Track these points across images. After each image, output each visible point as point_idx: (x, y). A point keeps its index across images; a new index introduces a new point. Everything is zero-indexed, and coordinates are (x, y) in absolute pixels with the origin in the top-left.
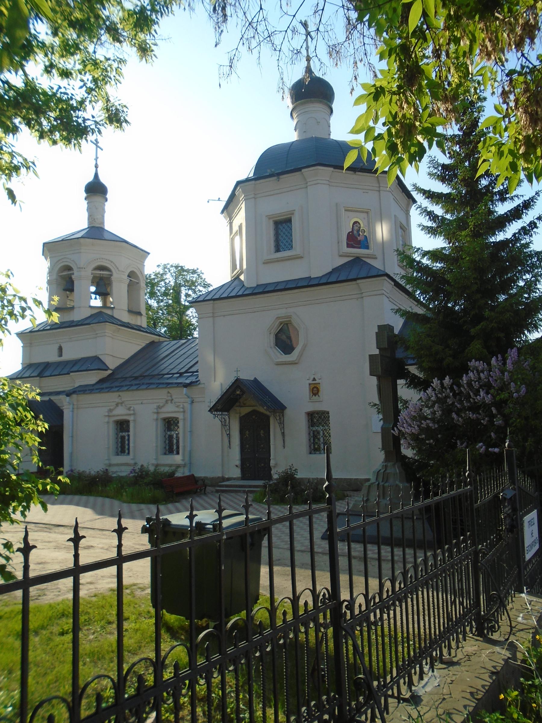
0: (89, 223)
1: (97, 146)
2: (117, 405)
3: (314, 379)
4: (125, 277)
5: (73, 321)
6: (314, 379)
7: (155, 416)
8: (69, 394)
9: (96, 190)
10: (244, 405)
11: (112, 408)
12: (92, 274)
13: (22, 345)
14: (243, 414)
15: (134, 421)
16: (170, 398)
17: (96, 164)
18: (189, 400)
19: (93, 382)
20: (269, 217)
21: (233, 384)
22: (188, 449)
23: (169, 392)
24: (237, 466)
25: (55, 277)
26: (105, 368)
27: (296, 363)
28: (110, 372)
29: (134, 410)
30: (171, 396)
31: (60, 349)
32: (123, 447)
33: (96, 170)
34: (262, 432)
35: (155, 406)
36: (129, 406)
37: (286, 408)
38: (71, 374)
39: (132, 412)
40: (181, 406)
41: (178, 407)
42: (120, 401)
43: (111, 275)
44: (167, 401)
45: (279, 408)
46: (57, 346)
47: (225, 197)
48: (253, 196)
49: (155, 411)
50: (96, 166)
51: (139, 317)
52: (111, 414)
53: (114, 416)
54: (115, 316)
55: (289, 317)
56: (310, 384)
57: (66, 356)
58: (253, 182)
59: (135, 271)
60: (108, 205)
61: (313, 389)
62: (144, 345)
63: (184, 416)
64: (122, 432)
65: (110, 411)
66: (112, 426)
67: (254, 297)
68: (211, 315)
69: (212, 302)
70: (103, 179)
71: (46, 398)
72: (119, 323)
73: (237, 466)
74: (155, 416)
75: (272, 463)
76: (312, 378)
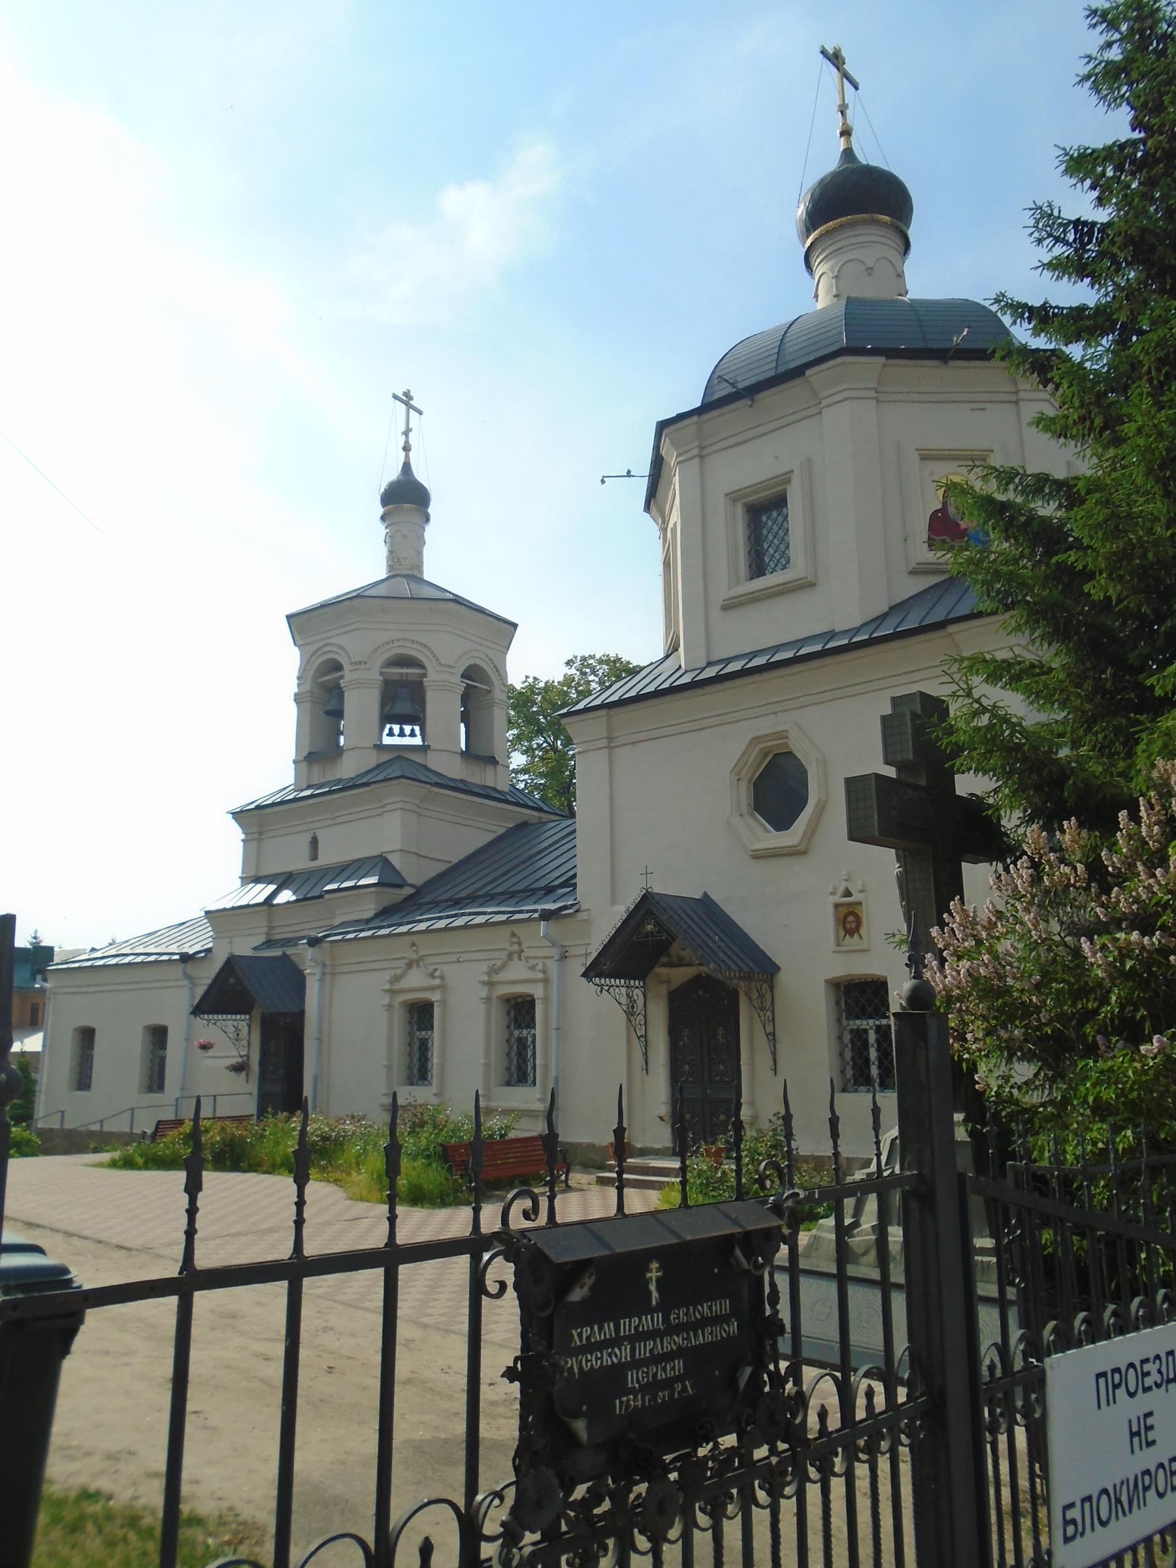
0: (390, 567)
1: (409, 406)
2: (409, 965)
3: (847, 893)
4: (457, 679)
5: (339, 781)
6: (847, 893)
7: (484, 992)
8: (314, 942)
9: (406, 499)
10: (681, 963)
12: (381, 674)
13: (243, 837)
14: (674, 985)
15: (443, 1002)
16: (516, 947)
17: (407, 442)
18: (555, 952)
19: (370, 914)
21: (638, 906)
22: (553, 1073)
23: (513, 935)
25: (307, 687)
26: (399, 882)
27: (804, 853)
28: (409, 891)
29: (442, 978)
30: (520, 944)
31: (314, 842)
32: (419, 1067)
33: (407, 457)
34: (720, 1031)
35: (485, 967)
37: (778, 968)
38: (327, 896)
39: (437, 982)
40: (540, 967)
41: (533, 968)
42: (414, 956)
43: (425, 675)
44: (510, 956)
45: (764, 970)
46: (306, 838)
47: (644, 467)
48: (696, 452)
49: (486, 978)
50: (407, 448)
51: (490, 770)
52: (397, 987)
53: (402, 991)
54: (431, 765)
55: (783, 735)
56: (837, 906)
57: (324, 860)
58: (695, 419)
59: (479, 662)
60: (429, 532)
61: (845, 917)
62: (501, 831)
63: (545, 991)
65: (396, 979)
66: (399, 1016)
67: (699, 691)
68: (604, 743)
69: (604, 712)
70: (421, 475)
71: (277, 952)
72: (436, 779)
73: (661, 1119)
74: (484, 992)
75: (745, 1114)
76: (840, 891)
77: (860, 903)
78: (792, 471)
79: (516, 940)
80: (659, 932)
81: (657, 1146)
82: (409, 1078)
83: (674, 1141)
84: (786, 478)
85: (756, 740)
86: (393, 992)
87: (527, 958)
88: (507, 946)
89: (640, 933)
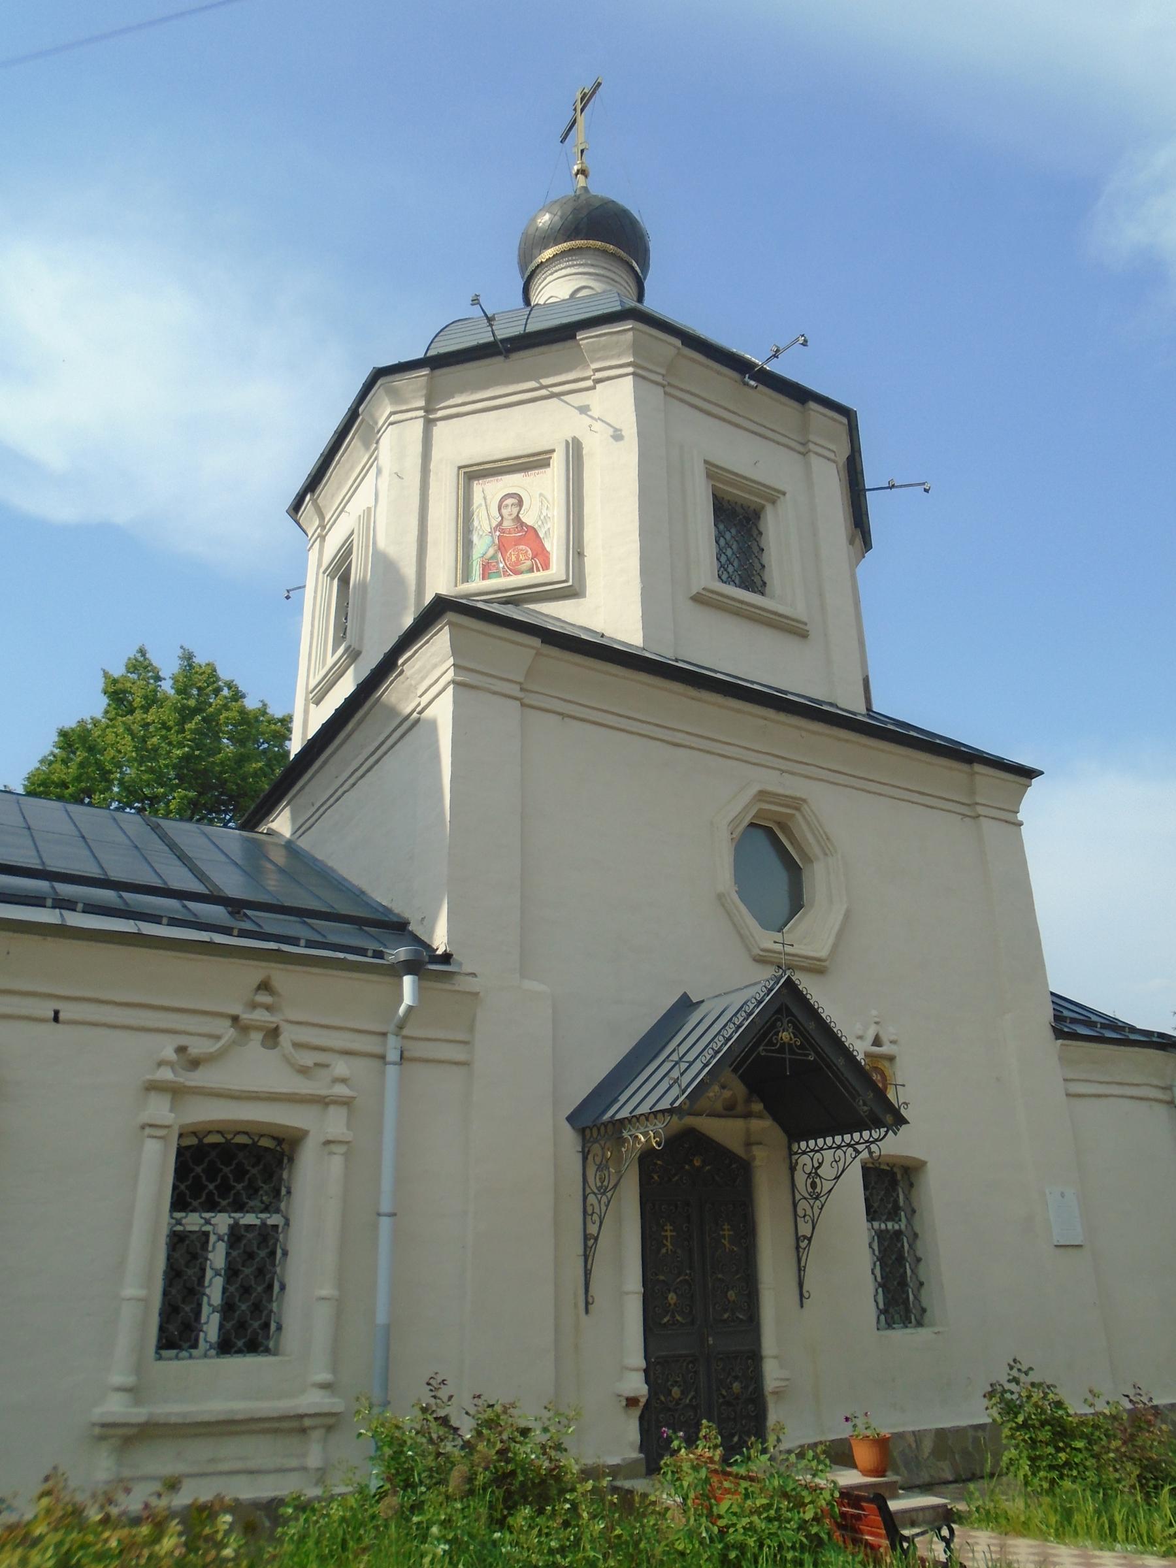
16: (260, 1016)
20: (713, 472)
24: (632, 1402)
41: (304, 1071)
55: (796, 803)
69: (536, 642)
75: (773, 1374)
77: (891, 1059)
78: (784, 494)
80: (801, 1047)
81: (613, 1460)
83: (642, 1449)
84: (774, 496)
85: (762, 795)
87: (297, 1045)
89: (770, 1043)
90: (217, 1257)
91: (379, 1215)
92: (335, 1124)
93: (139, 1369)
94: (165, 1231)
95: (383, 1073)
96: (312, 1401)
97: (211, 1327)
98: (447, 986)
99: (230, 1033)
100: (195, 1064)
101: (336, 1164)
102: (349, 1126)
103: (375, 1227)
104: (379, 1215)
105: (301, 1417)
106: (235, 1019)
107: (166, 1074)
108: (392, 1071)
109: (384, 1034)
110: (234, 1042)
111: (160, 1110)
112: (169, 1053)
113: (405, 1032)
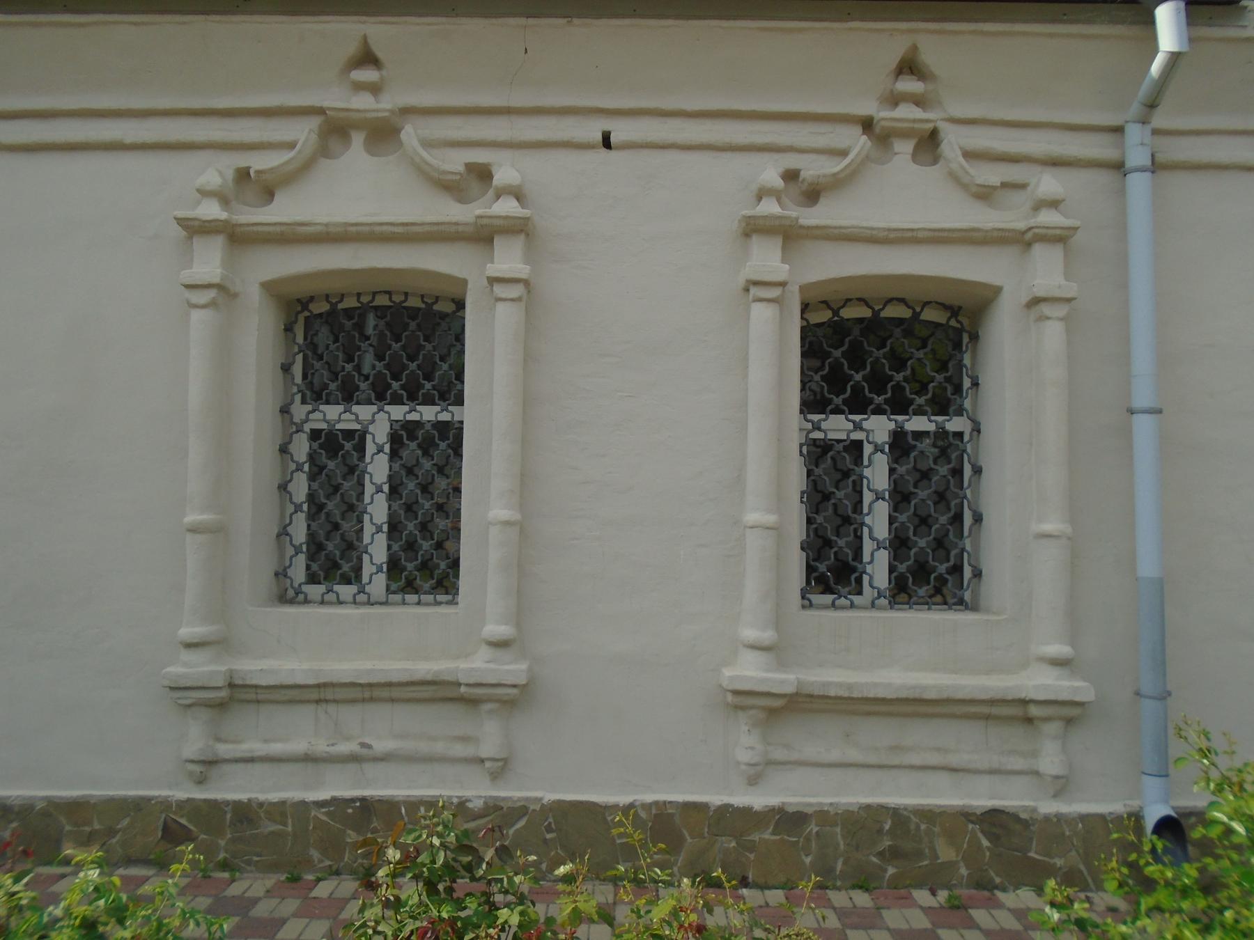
11: (259, 162)
29: (518, 195)
36: (454, 162)
39: (507, 207)
41: (984, 195)
42: (363, 102)
64: (349, 396)
66: (257, 336)
79: (909, 85)
82: (281, 574)
86: (239, 239)
87: (969, 155)
88: (867, 107)
90: (877, 473)
91: (1132, 412)
92: (1046, 272)
93: (778, 622)
94: (794, 440)
95: (1122, 192)
96: (1040, 682)
97: (878, 568)
98: (1232, 32)
99: (859, 142)
100: (812, 195)
101: (1053, 334)
102: (1068, 276)
103: (1126, 434)
104: (1132, 412)
105: (1024, 702)
106: (867, 125)
107: (770, 207)
108: (1139, 185)
109: (1119, 130)
110: (867, 159)
111: (767, 259)
112: (771, 175)
113: (1160, 120)
